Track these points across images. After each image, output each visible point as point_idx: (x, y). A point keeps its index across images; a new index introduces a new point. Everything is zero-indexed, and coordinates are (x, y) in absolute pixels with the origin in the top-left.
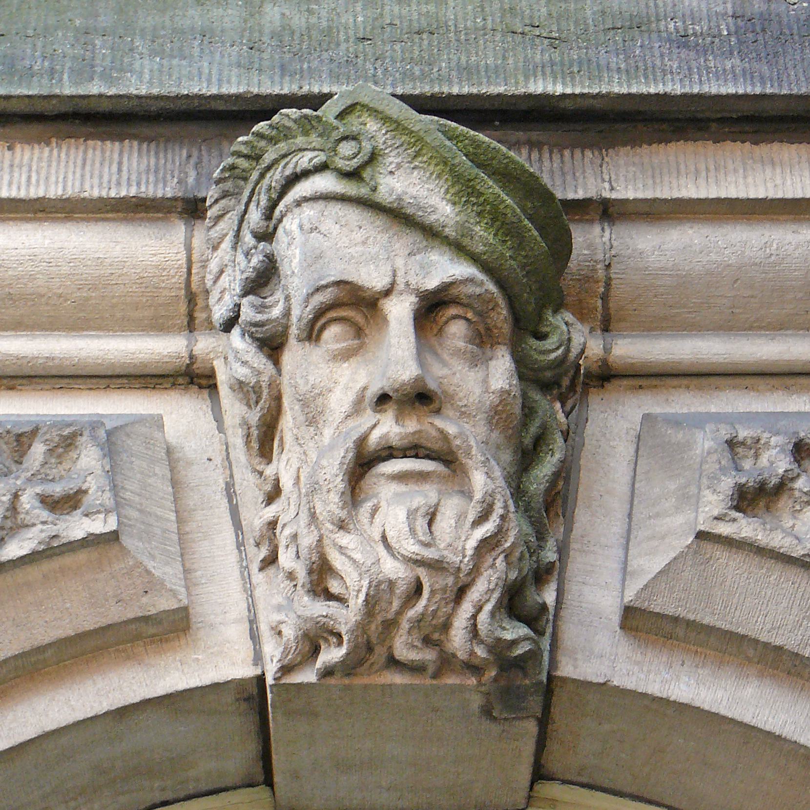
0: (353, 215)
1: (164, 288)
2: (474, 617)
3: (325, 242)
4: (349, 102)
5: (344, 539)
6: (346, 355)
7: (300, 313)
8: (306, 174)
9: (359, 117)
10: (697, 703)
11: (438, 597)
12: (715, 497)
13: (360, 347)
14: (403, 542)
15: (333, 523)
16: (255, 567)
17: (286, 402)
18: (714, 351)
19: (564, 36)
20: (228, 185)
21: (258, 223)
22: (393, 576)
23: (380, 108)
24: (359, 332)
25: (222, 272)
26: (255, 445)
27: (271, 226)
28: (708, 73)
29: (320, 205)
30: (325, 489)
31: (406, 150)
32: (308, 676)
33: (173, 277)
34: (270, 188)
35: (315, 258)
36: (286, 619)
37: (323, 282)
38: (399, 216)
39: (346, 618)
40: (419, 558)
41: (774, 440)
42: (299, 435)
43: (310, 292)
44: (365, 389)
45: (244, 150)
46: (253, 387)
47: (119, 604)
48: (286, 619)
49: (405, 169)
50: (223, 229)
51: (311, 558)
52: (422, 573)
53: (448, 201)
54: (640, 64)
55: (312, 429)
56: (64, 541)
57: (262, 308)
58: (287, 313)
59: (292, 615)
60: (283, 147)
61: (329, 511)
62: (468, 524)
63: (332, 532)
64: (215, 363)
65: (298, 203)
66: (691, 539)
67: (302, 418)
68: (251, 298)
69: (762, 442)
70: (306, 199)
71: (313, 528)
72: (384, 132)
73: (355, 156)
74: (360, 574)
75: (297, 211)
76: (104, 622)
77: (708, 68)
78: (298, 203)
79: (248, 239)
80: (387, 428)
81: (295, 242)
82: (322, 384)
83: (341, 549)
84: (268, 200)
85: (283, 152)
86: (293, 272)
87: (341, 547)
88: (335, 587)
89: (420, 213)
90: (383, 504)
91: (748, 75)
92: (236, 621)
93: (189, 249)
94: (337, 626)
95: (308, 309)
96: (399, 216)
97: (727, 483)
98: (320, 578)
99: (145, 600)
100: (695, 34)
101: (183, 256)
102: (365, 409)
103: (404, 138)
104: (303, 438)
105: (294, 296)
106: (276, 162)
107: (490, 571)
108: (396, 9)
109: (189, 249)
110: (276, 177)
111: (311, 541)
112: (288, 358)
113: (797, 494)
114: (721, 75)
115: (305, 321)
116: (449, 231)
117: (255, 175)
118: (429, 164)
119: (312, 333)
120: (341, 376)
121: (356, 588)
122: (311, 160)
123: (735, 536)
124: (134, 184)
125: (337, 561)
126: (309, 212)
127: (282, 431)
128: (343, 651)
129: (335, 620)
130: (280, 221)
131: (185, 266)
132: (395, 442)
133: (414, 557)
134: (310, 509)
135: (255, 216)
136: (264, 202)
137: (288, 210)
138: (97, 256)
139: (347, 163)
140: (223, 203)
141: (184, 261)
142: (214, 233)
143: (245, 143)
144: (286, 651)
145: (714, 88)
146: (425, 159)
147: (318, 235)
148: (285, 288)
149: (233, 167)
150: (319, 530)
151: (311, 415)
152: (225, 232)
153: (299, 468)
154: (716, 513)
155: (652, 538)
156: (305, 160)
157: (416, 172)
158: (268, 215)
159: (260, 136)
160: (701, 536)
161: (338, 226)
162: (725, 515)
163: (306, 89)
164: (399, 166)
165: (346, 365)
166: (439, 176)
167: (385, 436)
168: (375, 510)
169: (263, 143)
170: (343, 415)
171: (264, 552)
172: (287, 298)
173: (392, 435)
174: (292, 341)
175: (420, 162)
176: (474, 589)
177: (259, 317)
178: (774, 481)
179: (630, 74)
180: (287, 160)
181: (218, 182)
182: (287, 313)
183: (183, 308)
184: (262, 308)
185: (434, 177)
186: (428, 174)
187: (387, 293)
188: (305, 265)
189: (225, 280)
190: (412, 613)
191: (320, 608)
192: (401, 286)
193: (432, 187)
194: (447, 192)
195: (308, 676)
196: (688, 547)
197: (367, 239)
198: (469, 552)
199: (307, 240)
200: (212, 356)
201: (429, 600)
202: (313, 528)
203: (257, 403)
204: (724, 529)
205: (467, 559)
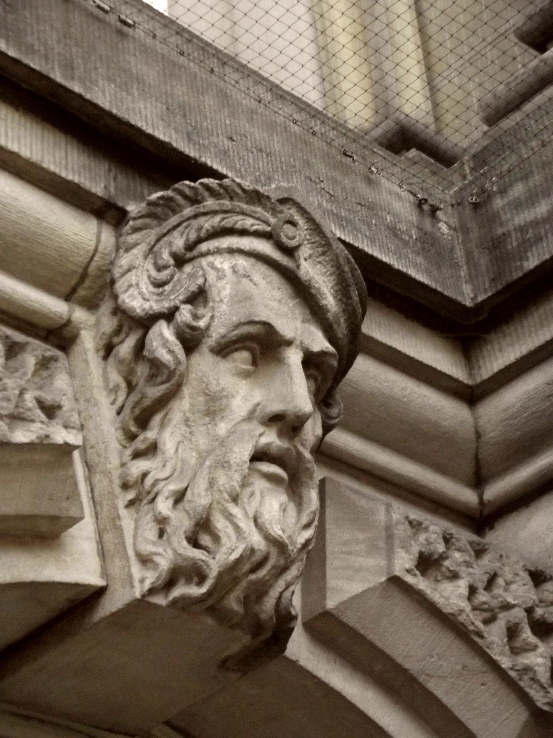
0: (275, 277)
1: (71, 262)
2: (281, 593)
3: (239, 286)
4: (286, 195)
5: (235, 510)
6: (246, 375)
7: (218, 332)
8: (243, 233)
9: (289, 209)
10: (344, 693)
11: (274, 571)
12: (408, 556)
13: (254, 372)
14: (274, 526)
15: (230, 496)
16: (121, 503)
17: (186, 391)
18: (355, 447)
19: (336, 194)
20: (159, 210)
21: (180, 250)
22: (256, 547)
23: (309, 210)
24: (255, 363)
25: (129, 270)
26: (137, 411)
27: (189, 255)
28: (409, 261)
29: (252, 260)
30: (234, 469)
31: (317, 247)
32: (160, 600)
33: (81, 256)
34: (200, 229)
35: (242, 298)
36: (164, 553)
37: (257, 319)
38: (302, 291)
39: (214, 565)
40: (281, 540)
41: (432, 528)
42: (192, 419)
43: (242, 320)
44: (258, 404)
45: (187, 191)
46: (170, 372)
47: (50, 502)
48: (164, 553)
49: (314, 260)
50: (138, 239)
51: (202, 515)
52: (274, 552)
53: (332, 294)
54: (376, 237)
55: (207, 419)
56: (52, 441)
57: (196, 317)
58: (208, 328)
59: (170, 552)
60: (227, 203)
61: (233, 486)
62: (300, 525)
63: (227, 501)
64: (83, 332)
65: (231, 251)
66: (383, 579)
67: (202, 408)
68: (188, 307)
69: (423, 526)
70: (240, 251)
71: (208, 493)
72: (306, 228)
73: (294, 238)
74: (237, 538)
75: (227, 256)
76: (36, 511)
77: (409, 258)
78: (231, 251)
79: (166, 257)
80: (270, 438)
81: (226, 279)
82: (229, 390)
83: (229, 517)
84: (197, 237)
85: (225, 208)
86: (221, 301)
87: (231, 514)
88: (205, 540)
89: (319, 297)
90: (258, 493)
91: (428, 272)
92: (88, 539)
93: (98, 240)
94: (207, 571)
95: (235, 332)
96: (302, 291)
97: (415, 549)
98: (201, 530)
99: (64, 504)
100: (400, 230)
101: (93, 244)
102: (253, 419)
103: (317, 239)
104: (194, 421)
105: (220, 319)
106: (214, 213)
107: (299, 563)
108: (247, 125)
109: (98, 240)
110: (208, 223)
111: (206, 502)
112: (196, 358)
113: (444, 569)
114: (415, 265)
115: (227, 340)
116: (330, 316)
117: (188, 211)
118: (328, 264)
119: (223, 350)
120: (241, 389)
121: (233, 548)
122: (252, 225)
123: (415, 586)
124: (77, 173)
125: (220, 523)
126: (242, 262)
127: (170, 410)
128: (204, 589)
129: (208, 566)
130: (203, 255)
131: (92, 252)
132: (273, 450)
133: (278, 538)
134: (209, 478)
135: (178, 242)
136: (193, 236)
137: (218, 251)
138: (38, 216)
139: (289, 241)
140: (147, 220)
141: (92, 248)
142: (132, 239)
143: (189, 187)
144: (158, 578)
145: (412, 272)
146: (327, 259)
147: (249, 282)
148: (213, 309)
149: (170, 199)
150: (212, 495)
151: (213, 409)
152: (139, 242)
153: (179, 442)
154: (407, 566)
155: (346, 568)
156: (248, 223)
157: (318, 266)
158: (190, 247)
159: (207, 188)
160: (395, 581)
161: (264, 282)
162: (412, 570)
163: (203, 159)
164: (310, 256)
165: (244, 382)
166: (331, 274)
167: (269, 445)
168: (252, 494)
169: (206, 194)
170: (240, 418)
171: (131, 495)
172: (212, 317)
173: (274, 445)
174: (204, 348)
175: (324, 260)
176: (288, 572)
177: (194, 324)
178: (436, 556)
179: (373, 241)
180: (225, 216)
181: (150, 204)
182: (208, 328)
183: (73, 282)
184: (196, 317)
185: (328, 273)
186: (325, 270)
187: (289, 343)
188: (235, 299)
189: (132, 277)
190: (253, 577)
191: (198, 554)
192: (298, 342)
193: (326, 280)
194: (332, 287)
195: (160, 600)
196: (381, 584)
197: (282, 299)
198: (299, 546)
199: (239, 282)
200: (82, 326)
201: (269, 571)
202: (208, 493)
203: (163, 383)
204: (409, 579)
205: (295, 550)
